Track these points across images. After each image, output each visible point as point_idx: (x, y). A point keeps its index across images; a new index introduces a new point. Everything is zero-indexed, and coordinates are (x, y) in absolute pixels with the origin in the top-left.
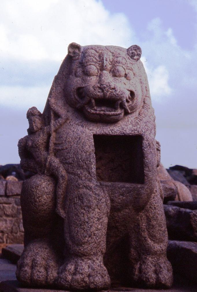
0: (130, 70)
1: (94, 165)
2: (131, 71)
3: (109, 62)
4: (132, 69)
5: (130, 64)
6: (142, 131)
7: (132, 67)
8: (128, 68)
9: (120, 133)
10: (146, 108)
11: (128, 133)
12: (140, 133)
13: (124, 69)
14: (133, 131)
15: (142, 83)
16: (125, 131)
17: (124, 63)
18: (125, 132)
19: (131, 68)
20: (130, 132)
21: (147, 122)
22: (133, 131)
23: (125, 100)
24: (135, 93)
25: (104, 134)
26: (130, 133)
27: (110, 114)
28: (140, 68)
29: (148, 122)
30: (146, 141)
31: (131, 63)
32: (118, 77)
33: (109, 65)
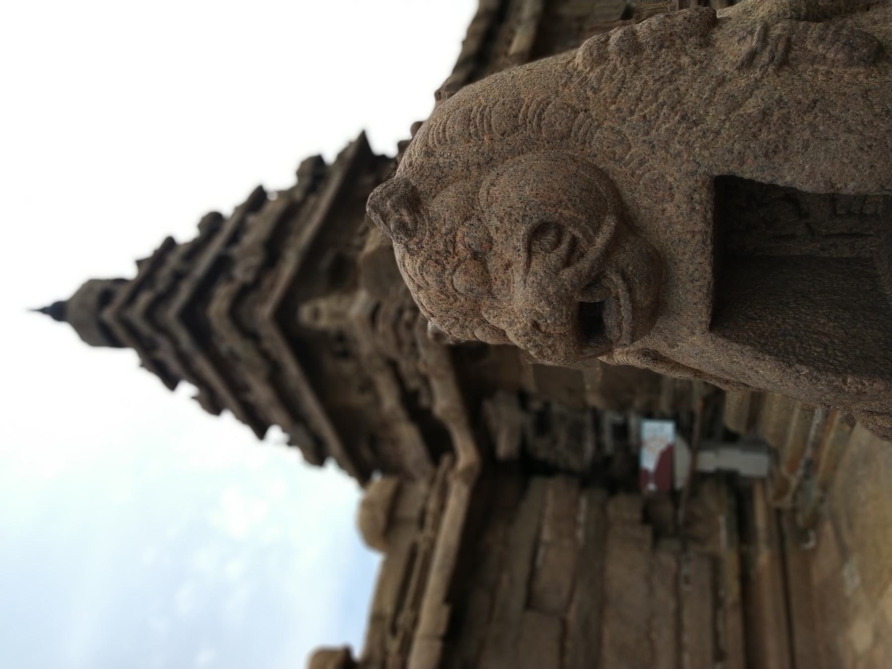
0: (454, 238)
1: (844, 382)
2: (460, 234)
3: (451, 304)
4: (450, 231)
5: (437, 238)
6: (694, 173)
7: (444, 230)
8: (451, 250)
9: (703, 253)
10: (586, 134)
11: (700, 226)
12: (704, 183)
13: (458, 266)
14: (693, 209)
15: (492, 159)
16: (694, 236)
17: (439, 267)
18: (698, 237)
19: (446, 235)
20: (697, 217)
21: (646, 138)
22: (693, 209)
23: (567, 274)
24: (535, 221)
25: (707, 301)
26: (705, 217)
27: (630, 308)
28: (437, 173)
29: (647, 133)
30: (742, 163)
31: (432, 235)
32: (490, 286)
33: (458, 303)
